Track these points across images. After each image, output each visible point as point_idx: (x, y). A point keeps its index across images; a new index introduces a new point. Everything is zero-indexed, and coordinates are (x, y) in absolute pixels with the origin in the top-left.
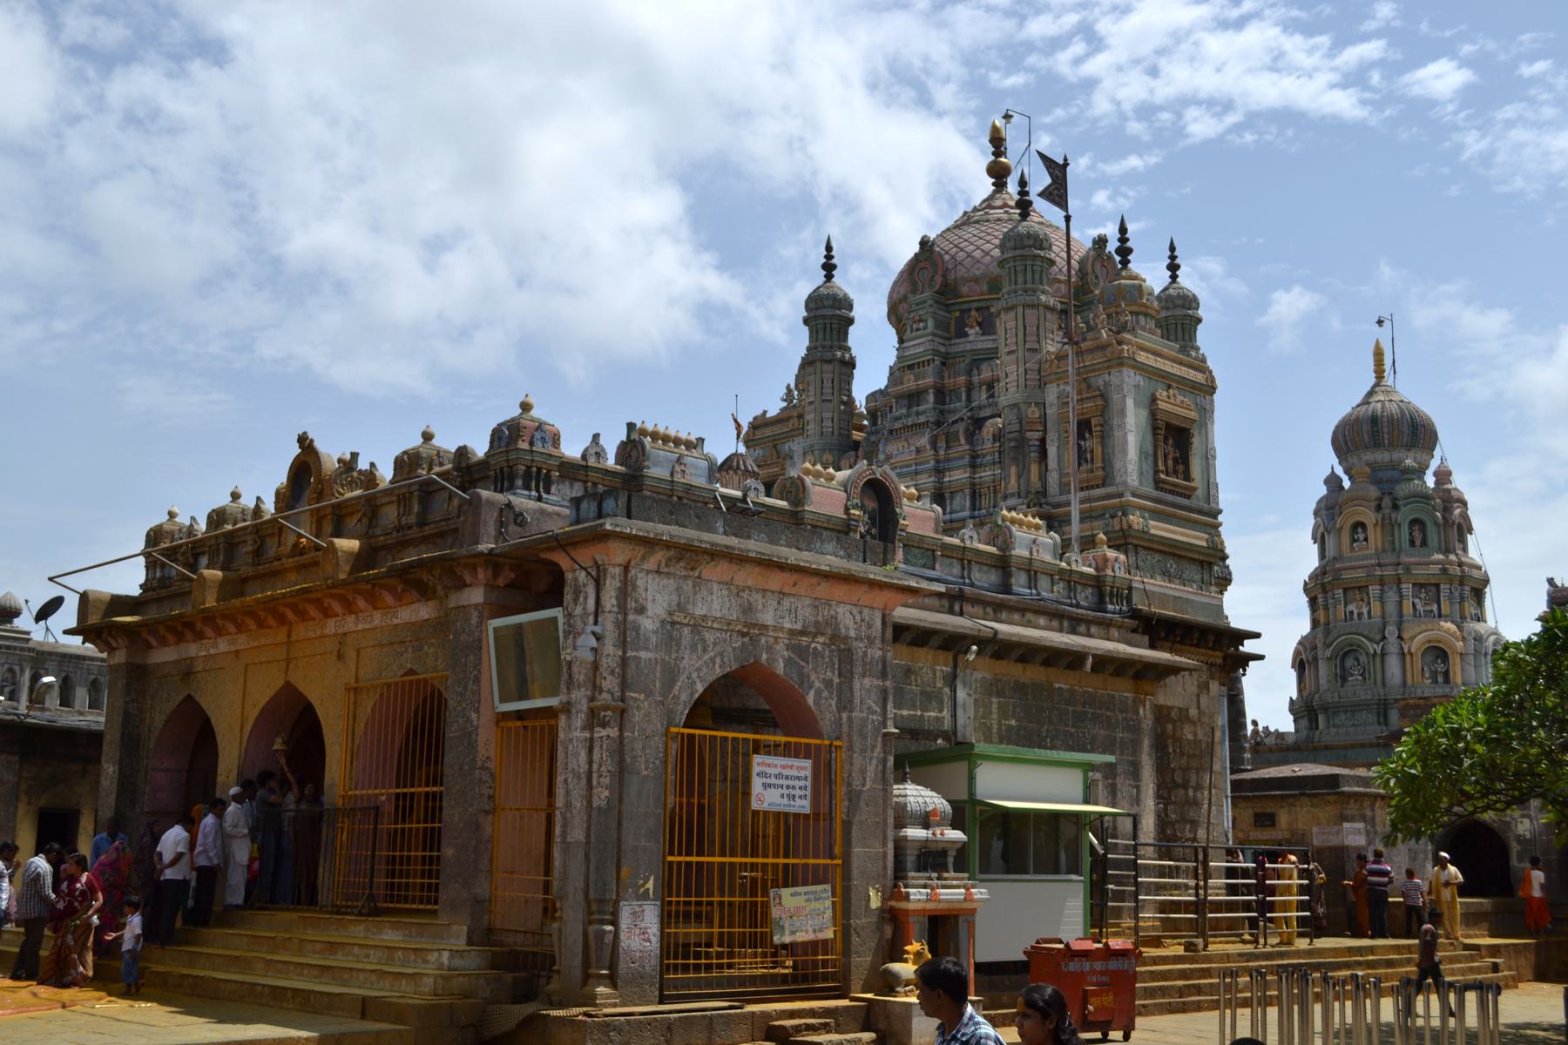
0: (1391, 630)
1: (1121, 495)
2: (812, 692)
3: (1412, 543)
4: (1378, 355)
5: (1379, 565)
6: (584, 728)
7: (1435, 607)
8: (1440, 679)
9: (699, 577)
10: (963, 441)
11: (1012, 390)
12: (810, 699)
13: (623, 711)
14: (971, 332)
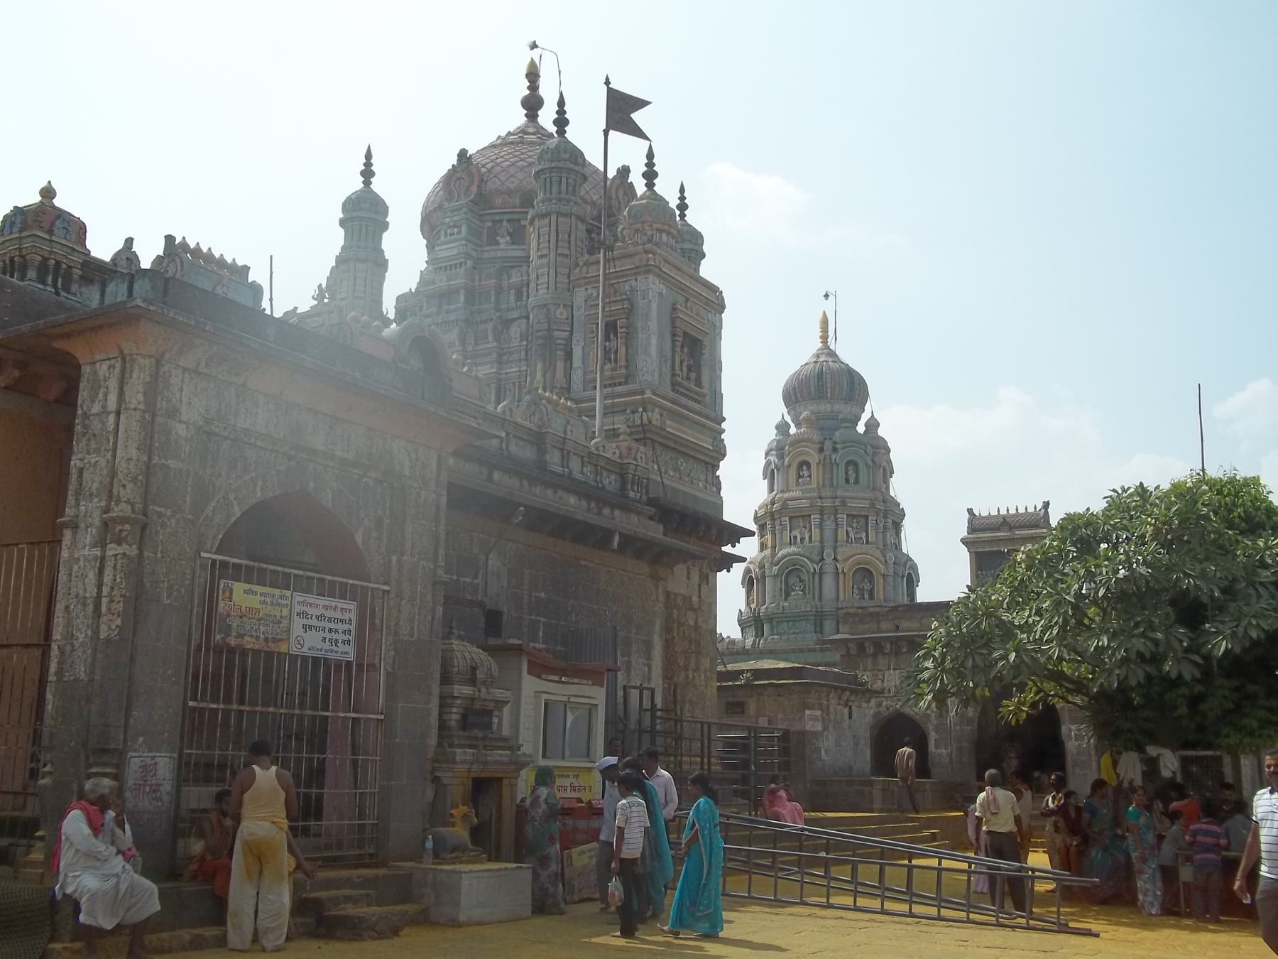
0: (828, 552)
2: (361, 530)
3: (847, 481)
4: (825, 323)
5: (820, 498)
7: (864, 535)
8: (867, 596)
9: (244, 385)
10: (490, 338)
12: (359, 538)
13: (144, 528)
14: (502, 241)
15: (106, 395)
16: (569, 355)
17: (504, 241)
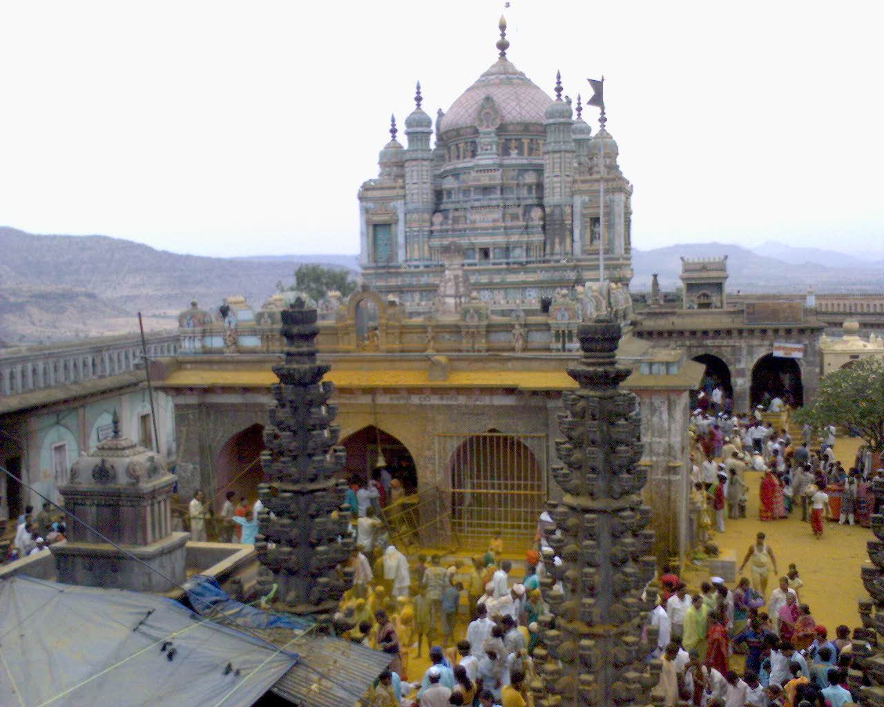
1: (618, 259)
16: (572, 231)
17: (514, 153)
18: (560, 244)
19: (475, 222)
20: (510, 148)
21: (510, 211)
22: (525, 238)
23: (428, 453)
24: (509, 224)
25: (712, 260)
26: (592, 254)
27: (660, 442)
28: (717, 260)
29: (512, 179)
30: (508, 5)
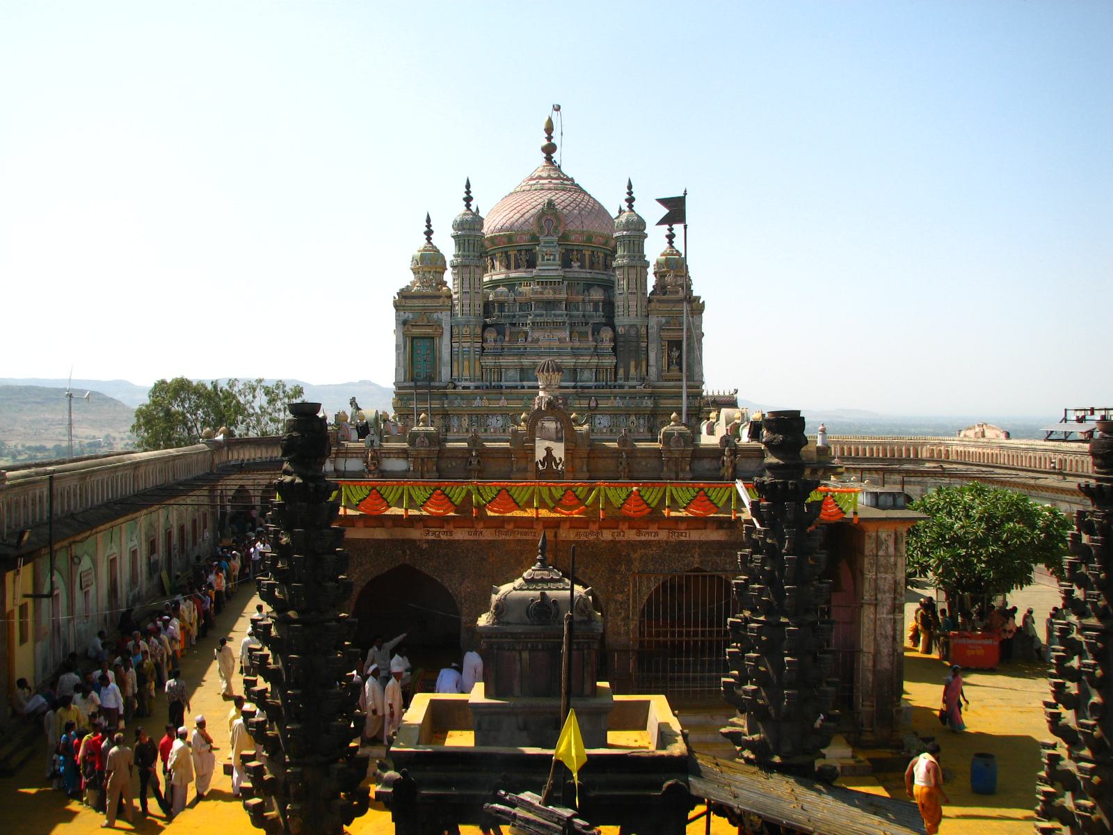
6: (889, 613)
11: (633, 314)
15: (887, 548)
17: (576, 265)
18: (636, 368)
19: (538, 340)
20: (571, 260)
21: (577, 329)
22: (595, 360)
23: (619, 597)
24: (577, 344)
25: (721, 394)
26: (669, 380)
27: (885, 578)
28: (727, 394)
29: (578, 293)
30: (557, 108)
